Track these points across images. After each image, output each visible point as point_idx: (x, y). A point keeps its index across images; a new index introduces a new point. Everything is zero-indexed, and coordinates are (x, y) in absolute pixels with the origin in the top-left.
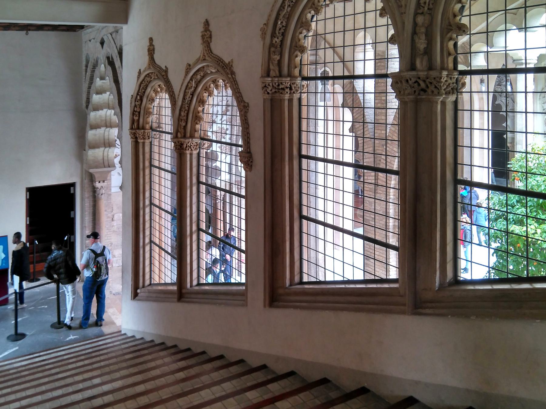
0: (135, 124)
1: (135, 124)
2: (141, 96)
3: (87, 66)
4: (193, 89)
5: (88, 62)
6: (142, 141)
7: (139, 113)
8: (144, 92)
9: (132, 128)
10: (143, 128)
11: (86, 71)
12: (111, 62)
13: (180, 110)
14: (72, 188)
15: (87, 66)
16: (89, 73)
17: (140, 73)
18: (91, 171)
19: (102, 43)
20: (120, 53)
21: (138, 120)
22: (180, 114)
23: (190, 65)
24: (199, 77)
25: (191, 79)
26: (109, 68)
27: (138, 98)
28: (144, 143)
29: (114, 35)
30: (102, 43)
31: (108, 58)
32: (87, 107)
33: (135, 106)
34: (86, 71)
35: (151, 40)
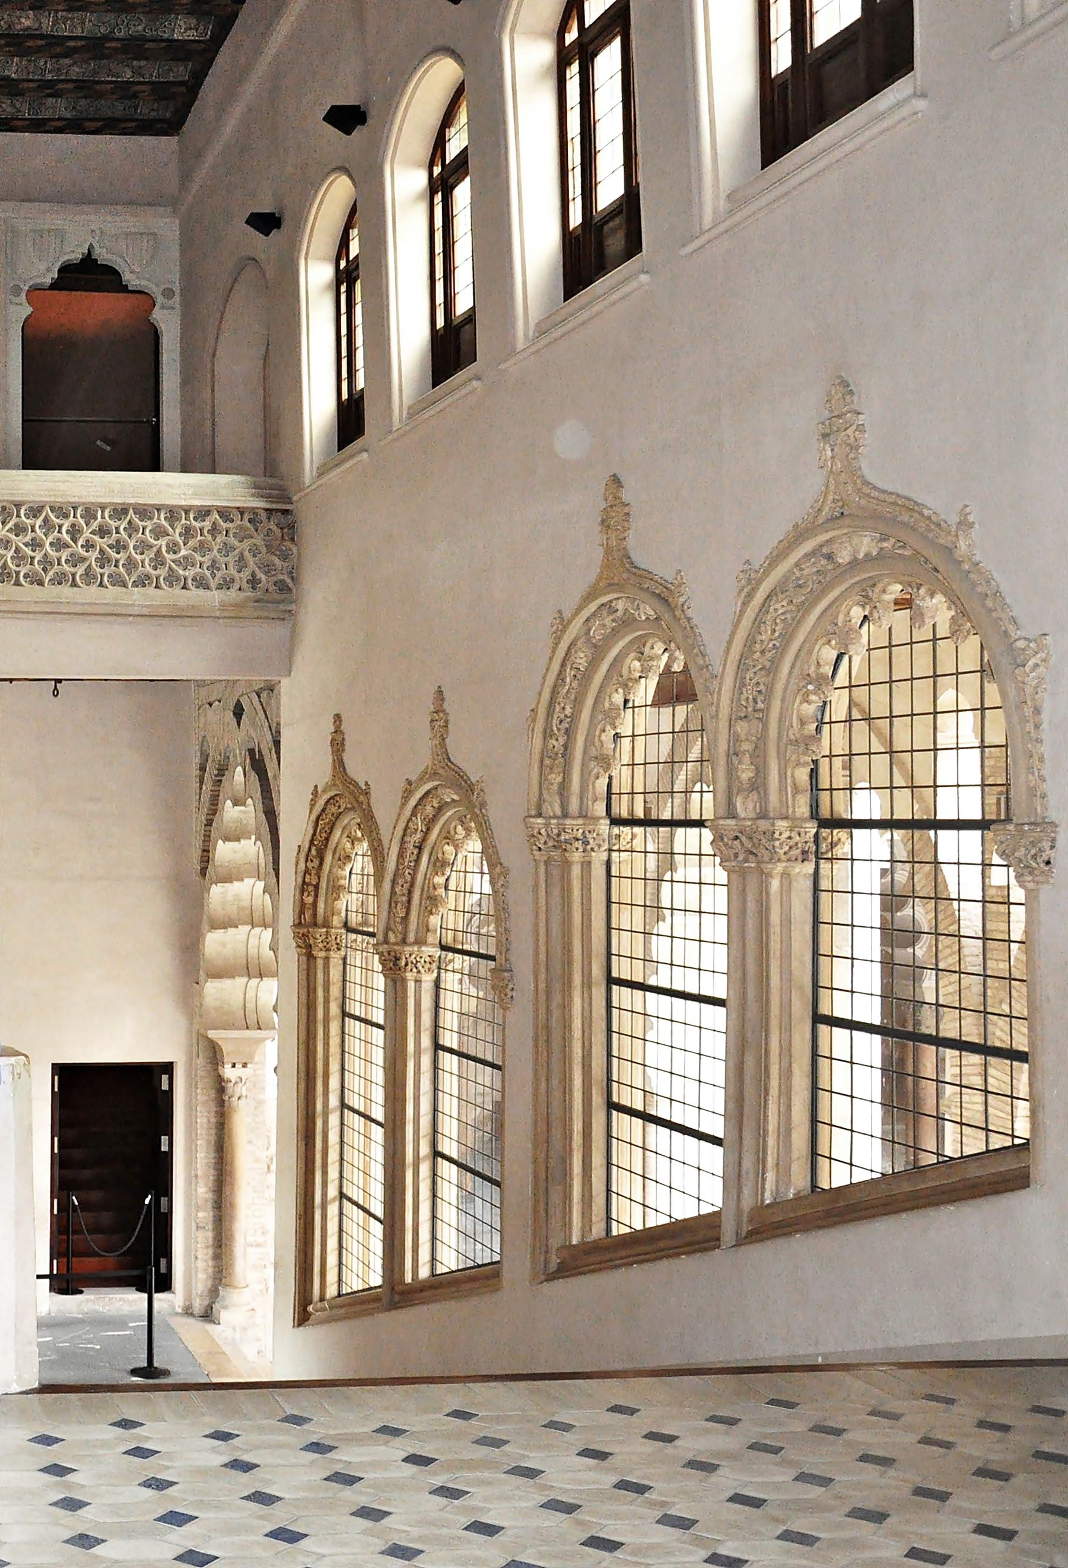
0: (308, 915)
1: (308, 915)
2: (318, 846)
3: (203, 769)
4: (419, 835)
5: (205, 757)
6: (322, 954)
7: (317, 887)
8: (327, 839)
9: (298, 924)
10: (327, 925)
11: (201, 782)
12: (257, 765)
13: (394, 882)
14: (165, 1078)
15: (203, 769)
16: (208, 787)
17: (315, 793)
18: (212, 1034)
19: (238, 712)
20: (277, 744)
21: (315, 904)
22: (393, 893)
23: (410, 783)
24: (429, 810)
25: (414, 813)
26: (253, 776)
27: (314, 852)
28: (327, 959)
29: (264, 695)
30: (238, 712)
31: (251, 751)
32: (203, 872)
33: (307, 871)
34: (201, 782)
35: (338, 718)
